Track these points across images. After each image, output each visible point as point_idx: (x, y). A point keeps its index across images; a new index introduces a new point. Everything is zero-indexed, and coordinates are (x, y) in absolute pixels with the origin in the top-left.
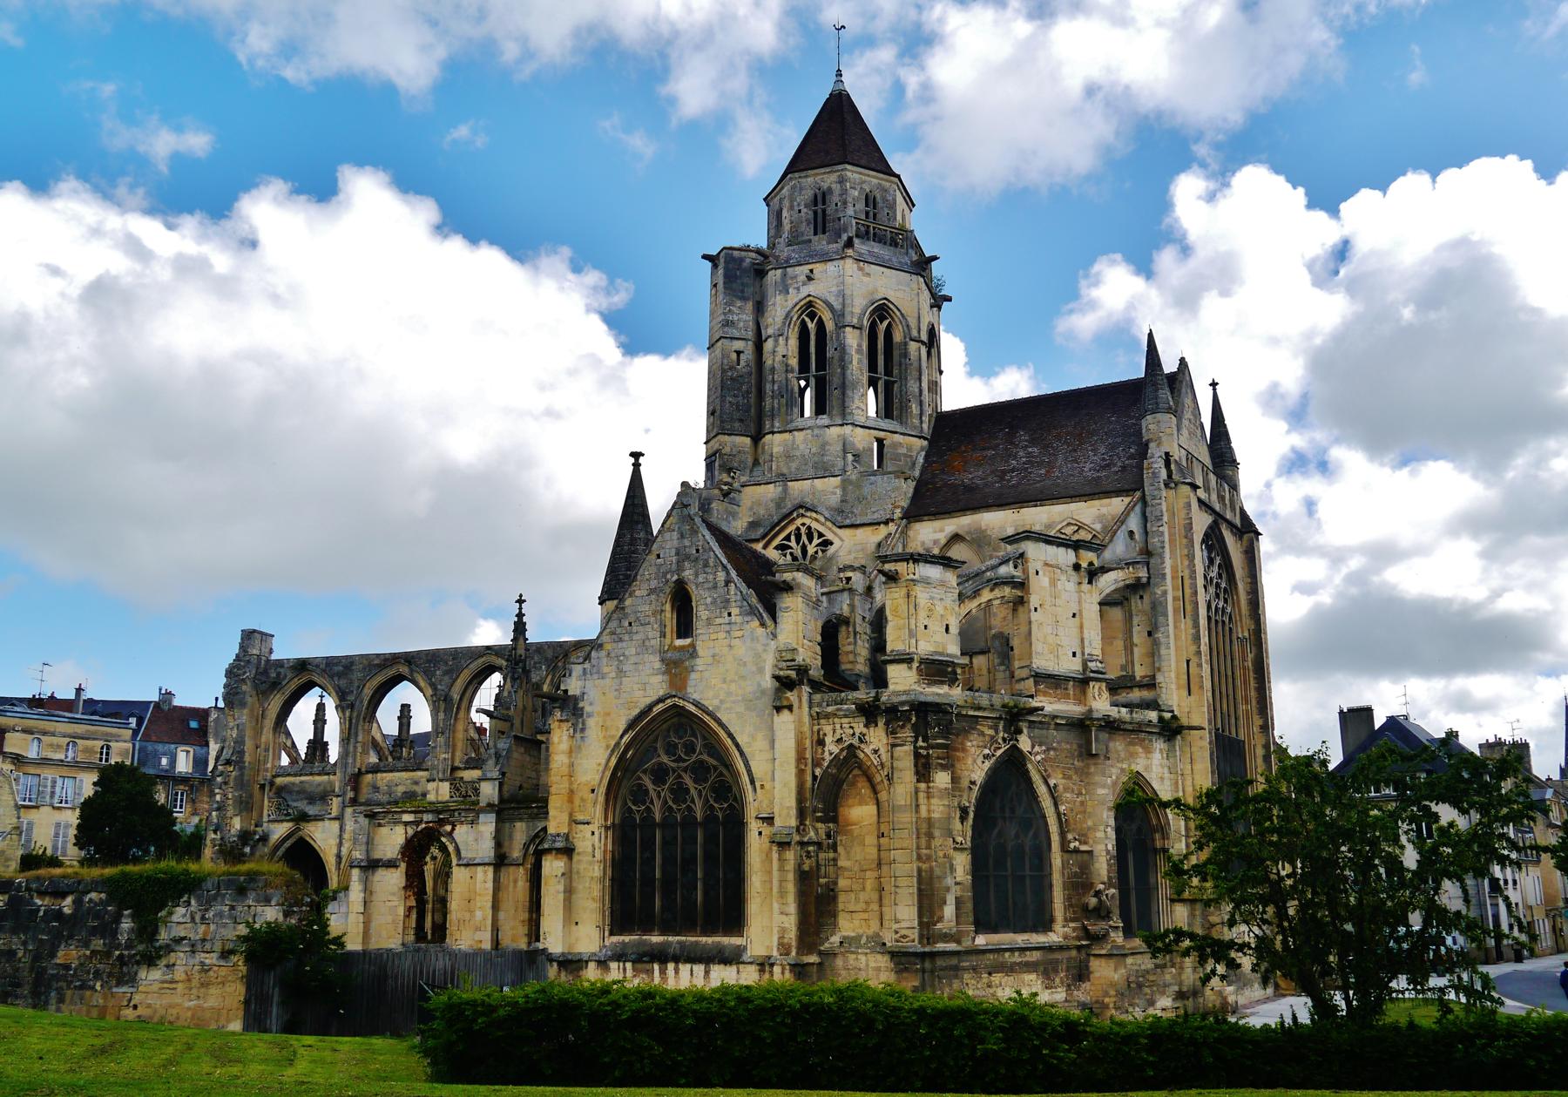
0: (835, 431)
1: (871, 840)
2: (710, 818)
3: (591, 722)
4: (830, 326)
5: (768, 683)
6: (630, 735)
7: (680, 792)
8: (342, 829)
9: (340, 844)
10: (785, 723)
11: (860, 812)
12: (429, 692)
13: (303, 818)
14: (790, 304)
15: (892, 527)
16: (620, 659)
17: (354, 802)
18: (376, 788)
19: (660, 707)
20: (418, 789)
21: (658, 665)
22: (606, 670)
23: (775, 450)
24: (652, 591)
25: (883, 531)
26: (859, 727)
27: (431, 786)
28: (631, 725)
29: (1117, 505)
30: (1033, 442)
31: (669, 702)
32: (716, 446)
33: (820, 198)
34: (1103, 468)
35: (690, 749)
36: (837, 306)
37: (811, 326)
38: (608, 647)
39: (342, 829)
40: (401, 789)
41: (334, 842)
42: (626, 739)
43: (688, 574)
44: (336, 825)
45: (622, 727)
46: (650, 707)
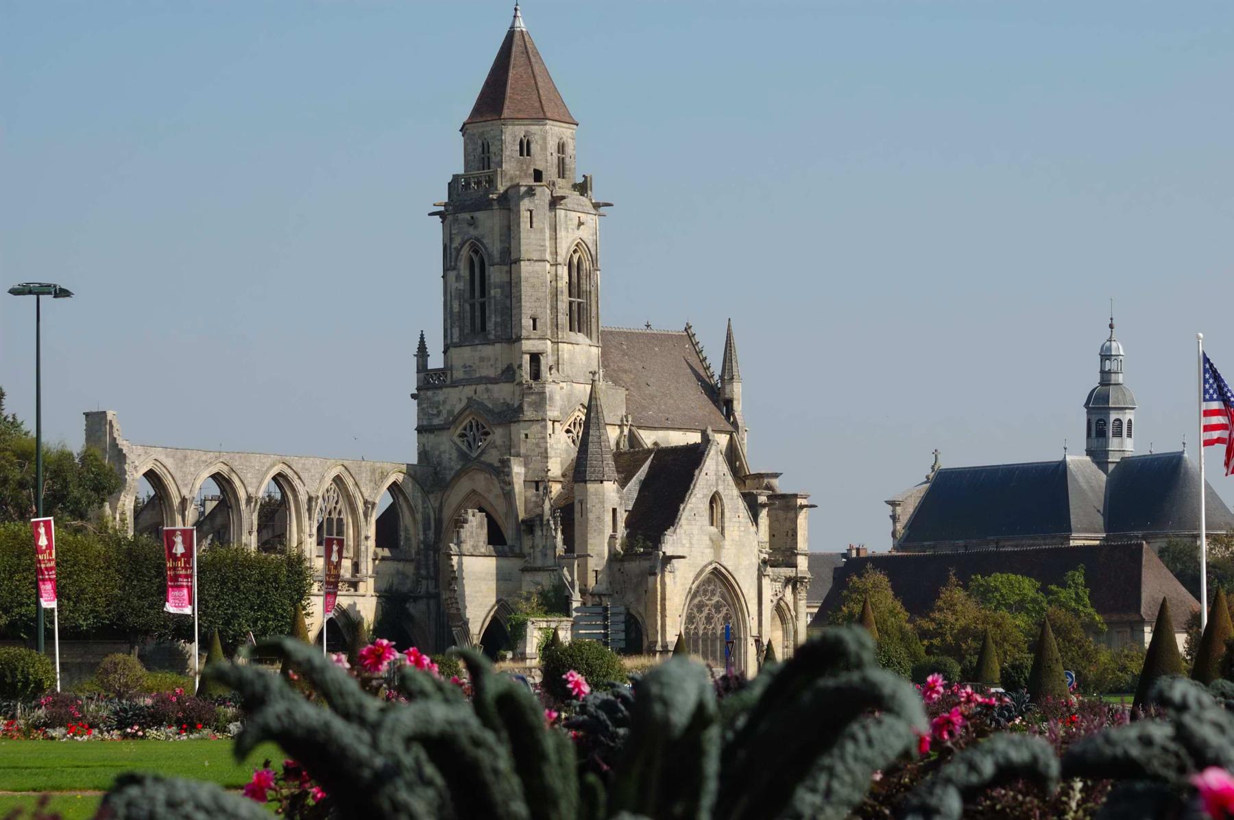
3: (677, 573)
4: (586, 265)
6: (697, 583)
14: (570, 240)
16: (690, 536)
19: (710, 568)
21: (708, 542)
22: (684, 542)
23: (566, 356)
24: (705, 496)
28: (696, 578)
31: (714, 565)
33: (561, 148)
35: (713, 594)
36: (593, 253)
38: (685, 527)
42: (694, 586)
45: (692, 576)
46: (706, 566)
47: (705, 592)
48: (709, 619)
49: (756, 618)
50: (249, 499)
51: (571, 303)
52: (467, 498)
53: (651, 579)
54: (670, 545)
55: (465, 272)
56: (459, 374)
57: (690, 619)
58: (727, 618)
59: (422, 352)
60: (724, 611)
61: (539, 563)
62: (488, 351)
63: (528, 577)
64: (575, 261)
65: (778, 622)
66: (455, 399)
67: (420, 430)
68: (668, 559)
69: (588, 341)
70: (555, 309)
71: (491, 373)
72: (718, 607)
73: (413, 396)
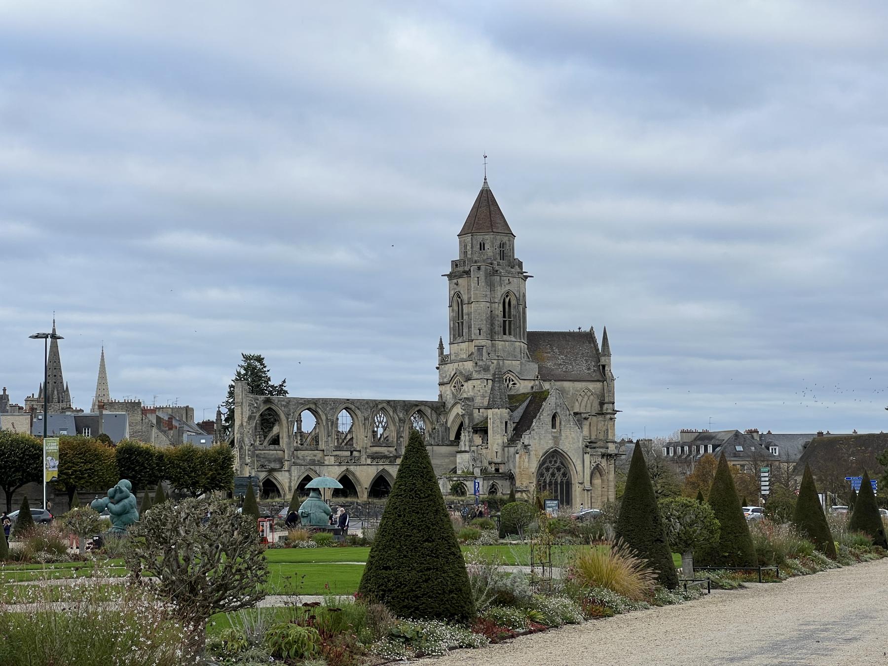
0: (518, 344)
1: (600, 489)
2: (562, 482)
4: (513, 302)
5: (581, 444)
7: (553, 475)
8: (290, 475)
9: (290, 482)
10: (587, 457)
11: (597, 481)
12: (324, 418)
13: (272, 470)
14: (503, 291)
15: (537, 382)
17: (295, 464)
18: (298, 458)
20: (316, 459)
25: (533, 382)
26: (600, 459)
27: (326, 458)
29: (599, 385)
30: (561, 353)
32: (483, 344)
33: (502, 245)
34: (589, 369)
35: (556, 462)
37: (507, 300)
39: (290, 475)
40: (309, 458)
41: (287, 481)
43: (558, 411)
44: (287, 474)
47: (550, 462)
48: (553, 475)
49: (581, 474)
50: (327, 419)
51: (504, 322)
52: (456, 417)
53: (517, 456)
54: (526, 439)
55: (456, 308)
56: (453, 357)
57: (542, 475)
58: (564, 475)
59: (441, 347)
60: (562, 471)
61: (463, 449)
62: (464, 346)
63: (459, 456)
64: (507, 300)
65: (598, 474)
66: (450, 369)
67: (440, 384)
68: (526, 447)
69: (513, 339)
70: (492, 324)
71: (464, 356)
72: (559, 469)
73: (438, 368)
